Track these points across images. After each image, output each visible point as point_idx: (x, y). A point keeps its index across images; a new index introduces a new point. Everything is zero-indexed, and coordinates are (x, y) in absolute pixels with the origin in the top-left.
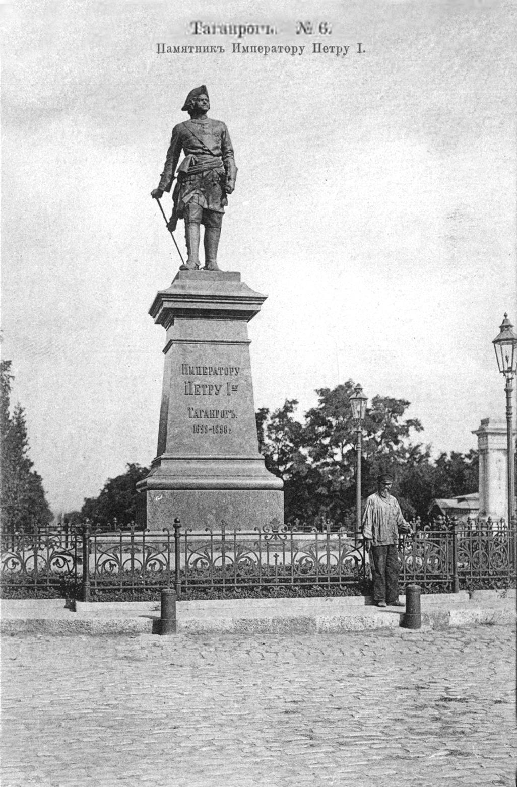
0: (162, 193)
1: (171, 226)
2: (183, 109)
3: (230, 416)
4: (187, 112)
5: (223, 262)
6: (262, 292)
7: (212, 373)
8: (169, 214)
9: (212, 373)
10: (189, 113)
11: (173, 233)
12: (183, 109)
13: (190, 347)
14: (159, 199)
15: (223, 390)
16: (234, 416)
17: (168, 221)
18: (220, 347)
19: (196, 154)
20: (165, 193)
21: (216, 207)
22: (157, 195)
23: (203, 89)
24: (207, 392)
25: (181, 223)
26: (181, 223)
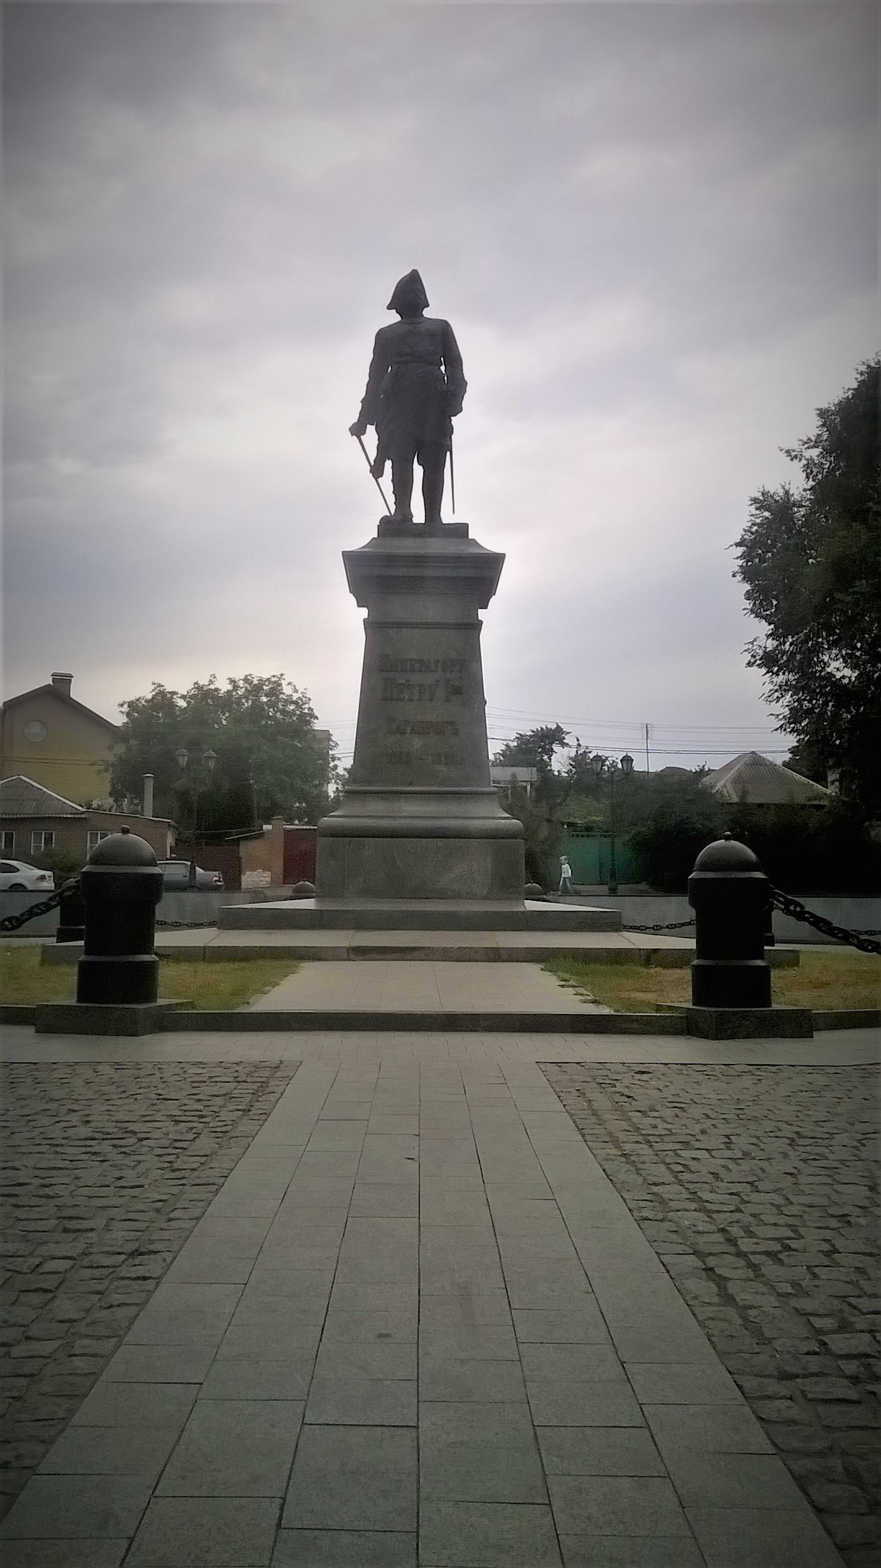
1: (377, 471)
2: (389, 308)
4: (395, 310)
5: (447, 516)
8: (373, 454)
11: (379, 480)
12: (389, 308)
14: (362, 436)
16: (456, 733)
17: (372, 463)
22: (358, 430)
24: (416, 696)
25: (388, 464)
26: (388, 464)
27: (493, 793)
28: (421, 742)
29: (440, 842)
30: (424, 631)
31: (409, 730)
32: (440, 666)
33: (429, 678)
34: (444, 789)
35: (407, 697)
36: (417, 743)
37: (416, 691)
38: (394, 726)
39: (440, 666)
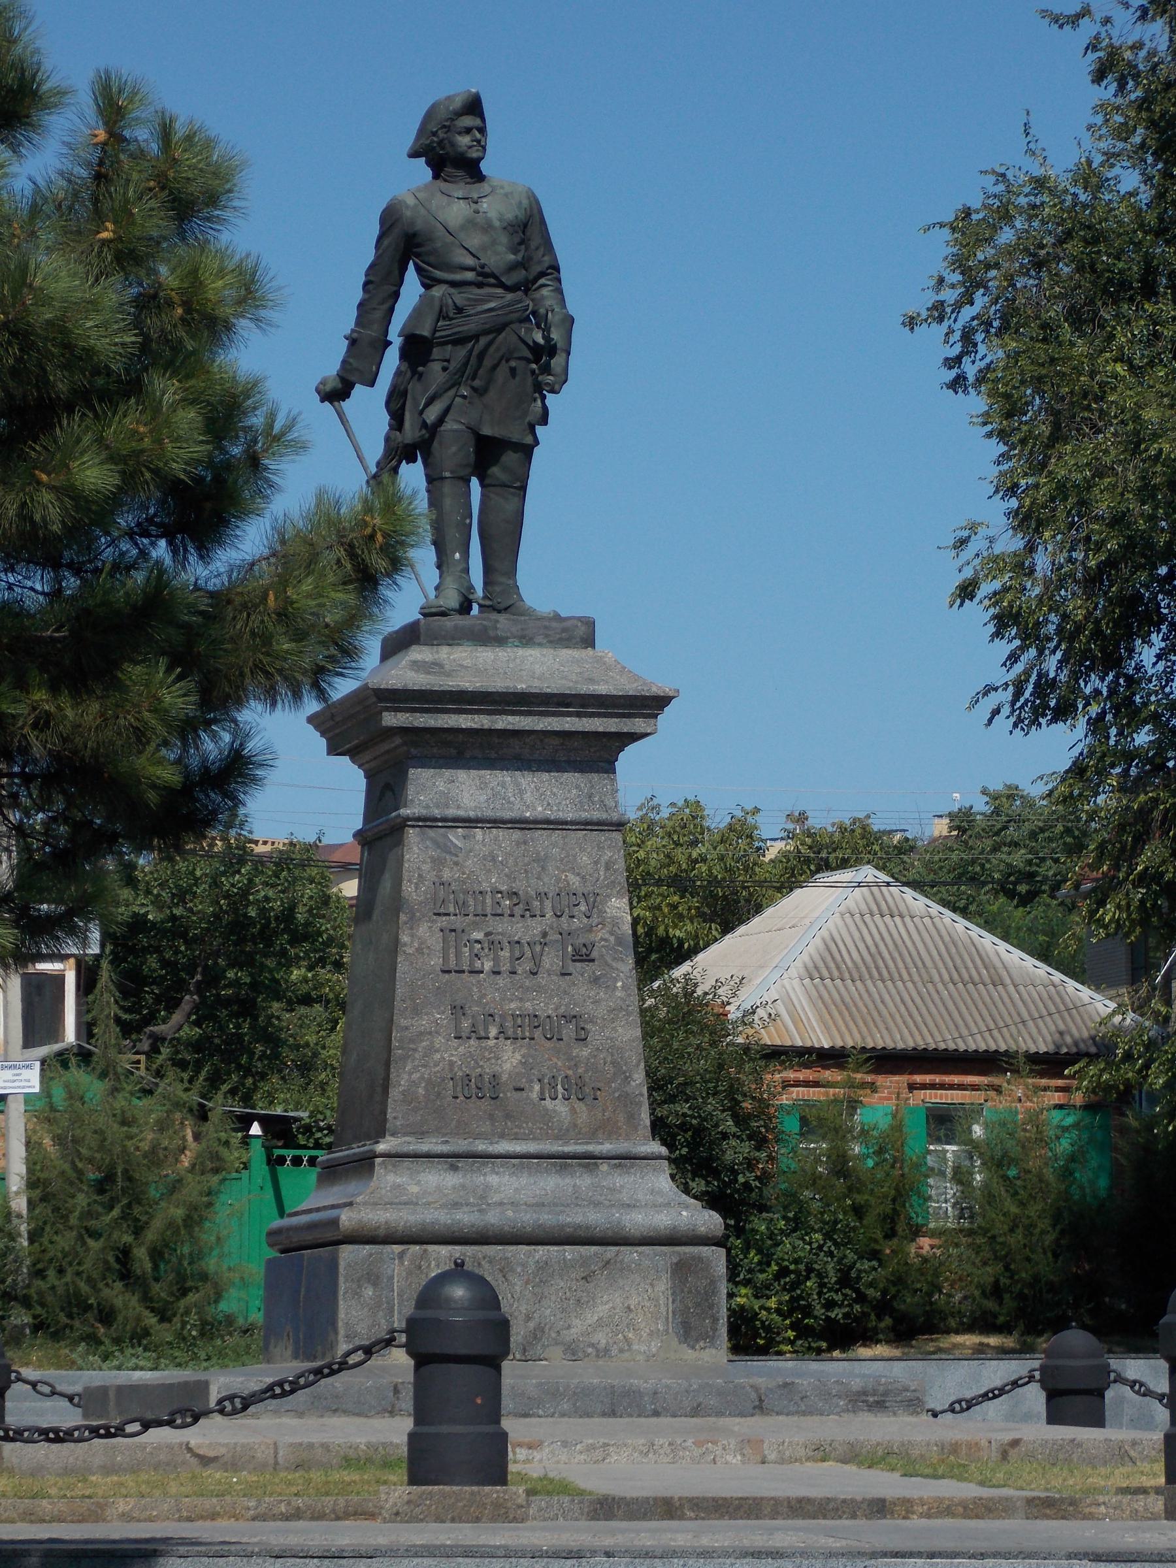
0: (352, 386)
2: (414, 154)
3: (569, 1031)
6: (659, 684)
7: (518, 910)
8: (375, 451)
9: (518, 910)
10: (428, 163)
12: (414, 154)
13: (455, 837)
15: (551, 960)
18: (542, 840)
19: (453, 284)
20: (359, 390)
21: (515, 433)
23: (474, 106)
27: (659, 1157)
28: (518, 1056)
29: (569, 1252)
30: (517, 835)
31: (493, 1032)
32: (548, 904)
33: (526, 930)
34: (568, 1149)
35: (488, 965)
36: (510, 1059)
37: (505, 954)
38: (466, 1024)
39: (548, 904)
